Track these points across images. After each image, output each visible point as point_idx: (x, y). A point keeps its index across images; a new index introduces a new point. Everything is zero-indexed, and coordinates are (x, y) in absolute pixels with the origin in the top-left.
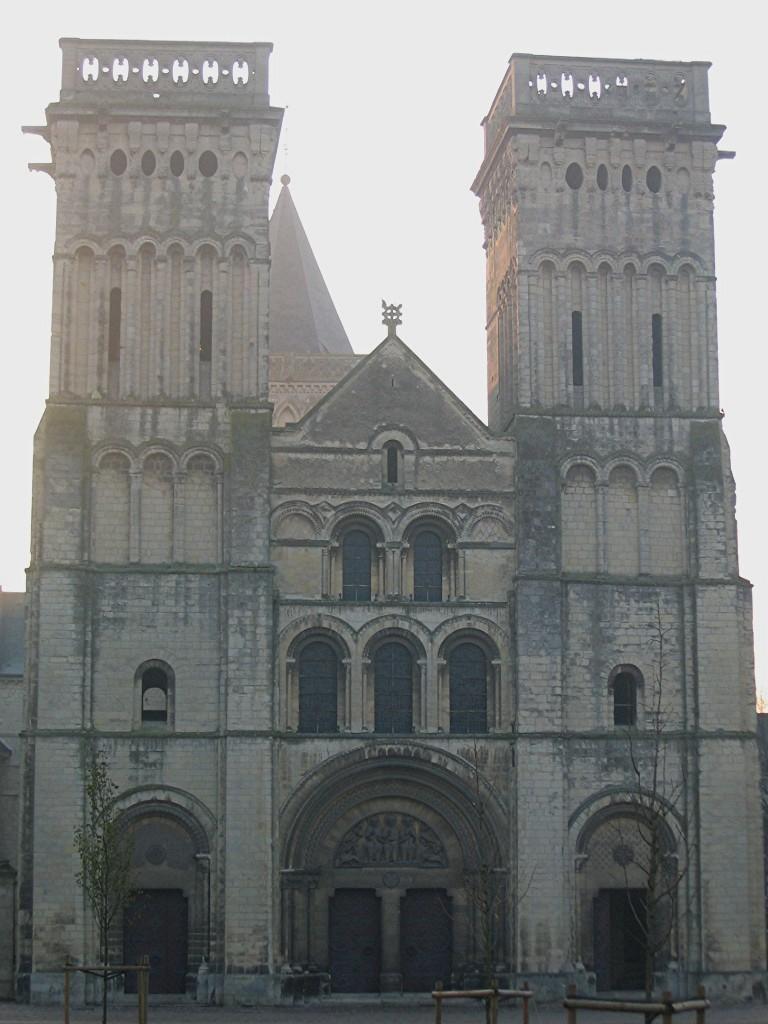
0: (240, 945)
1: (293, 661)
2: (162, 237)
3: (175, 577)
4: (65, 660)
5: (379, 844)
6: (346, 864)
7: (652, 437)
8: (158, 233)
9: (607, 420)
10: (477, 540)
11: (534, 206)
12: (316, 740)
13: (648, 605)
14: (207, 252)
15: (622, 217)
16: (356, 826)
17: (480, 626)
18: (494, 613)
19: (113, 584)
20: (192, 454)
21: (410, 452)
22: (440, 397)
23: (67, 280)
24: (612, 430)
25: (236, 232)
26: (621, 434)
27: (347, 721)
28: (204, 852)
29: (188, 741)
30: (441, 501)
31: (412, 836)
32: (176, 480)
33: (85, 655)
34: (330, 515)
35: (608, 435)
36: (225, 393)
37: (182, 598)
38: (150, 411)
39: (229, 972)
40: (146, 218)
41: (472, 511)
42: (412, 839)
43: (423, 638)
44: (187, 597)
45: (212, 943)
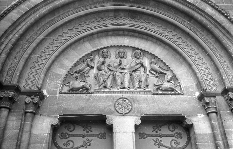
6: (74, 90)
16: (87, 56)
31: (142, 65)
42: (142, 69)
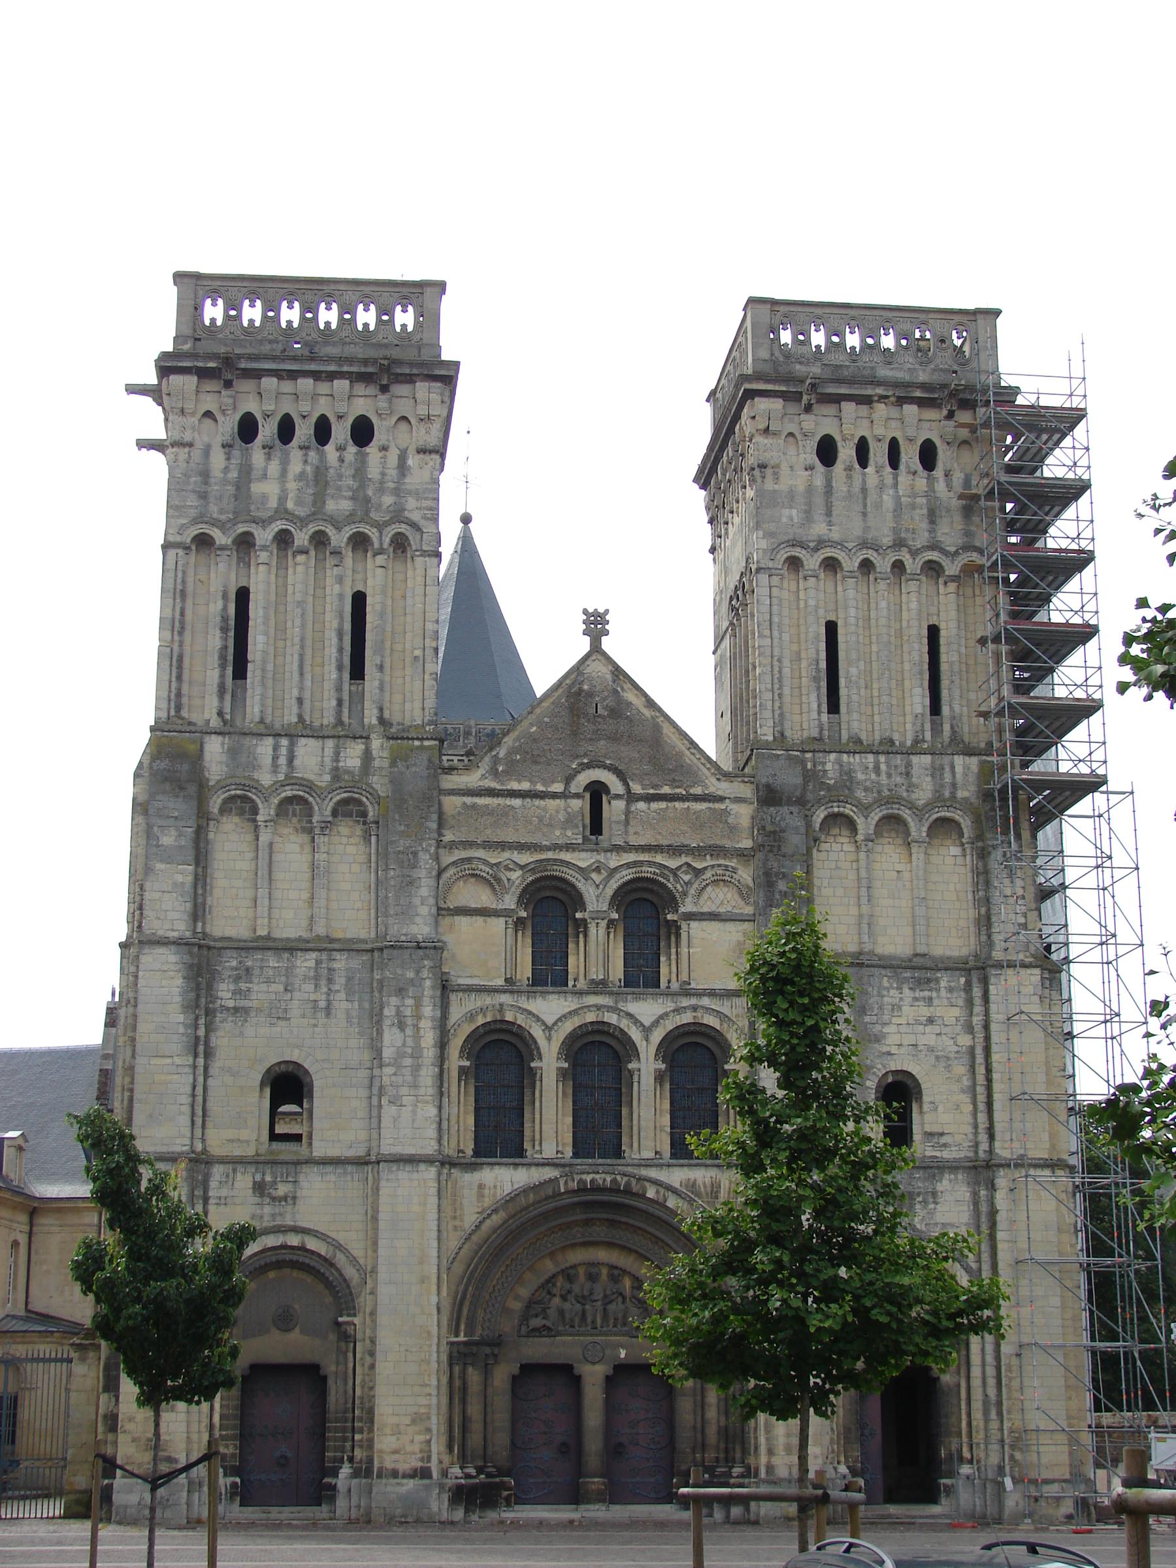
0: (394, 1439)
1: (467, 1063)
2: (303, 522)
3: (314, 955)
4: (169, 1061)
5: (578, 1306)
6: (537, 1332)
7: (929, 779)
8: (298, 517)
9: (871, 757)
10: (705, 909)
11: (776, 487)
12: (497, 1167)
13: (927, 994)
14: (360, 542)
15: (888, 500)
16: (548, 1281)
17: (711, 1021)
18: (727, 1003)
19: (234, 963)
20: (338, 798)
21: (618, 797)
22: (657, 728)
23: (180, 575)
24: (877, 769)
25: (398, 515)
26: (889, 776)
27: (537, 1143)
28: (349, 1315)
29: (329, 1169)
30: (659, 859)
31: (621, 1294)
32: (317, 831)
33: (196, 1055)
34: (516, 875)
35: (873, 776)
36: (382, 721)
37: (323, 982)
38: (284, 742)
39: (380, 1476)
40: (283, 499)
41: (698, 872)
42: (620, 1299)
43: (635, 1034)
44: (330, 981)
45: (357, 1437)
